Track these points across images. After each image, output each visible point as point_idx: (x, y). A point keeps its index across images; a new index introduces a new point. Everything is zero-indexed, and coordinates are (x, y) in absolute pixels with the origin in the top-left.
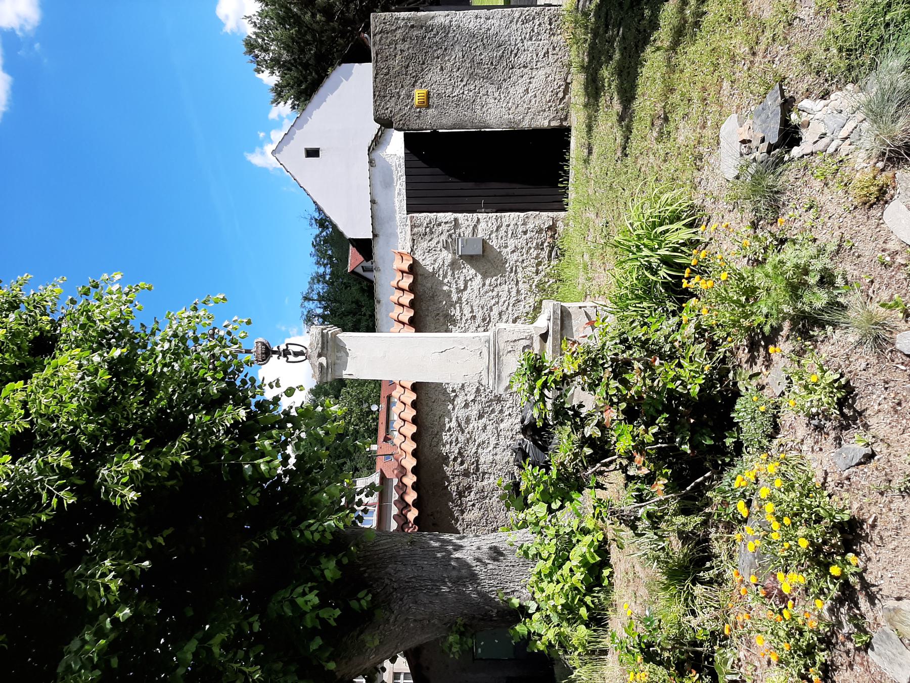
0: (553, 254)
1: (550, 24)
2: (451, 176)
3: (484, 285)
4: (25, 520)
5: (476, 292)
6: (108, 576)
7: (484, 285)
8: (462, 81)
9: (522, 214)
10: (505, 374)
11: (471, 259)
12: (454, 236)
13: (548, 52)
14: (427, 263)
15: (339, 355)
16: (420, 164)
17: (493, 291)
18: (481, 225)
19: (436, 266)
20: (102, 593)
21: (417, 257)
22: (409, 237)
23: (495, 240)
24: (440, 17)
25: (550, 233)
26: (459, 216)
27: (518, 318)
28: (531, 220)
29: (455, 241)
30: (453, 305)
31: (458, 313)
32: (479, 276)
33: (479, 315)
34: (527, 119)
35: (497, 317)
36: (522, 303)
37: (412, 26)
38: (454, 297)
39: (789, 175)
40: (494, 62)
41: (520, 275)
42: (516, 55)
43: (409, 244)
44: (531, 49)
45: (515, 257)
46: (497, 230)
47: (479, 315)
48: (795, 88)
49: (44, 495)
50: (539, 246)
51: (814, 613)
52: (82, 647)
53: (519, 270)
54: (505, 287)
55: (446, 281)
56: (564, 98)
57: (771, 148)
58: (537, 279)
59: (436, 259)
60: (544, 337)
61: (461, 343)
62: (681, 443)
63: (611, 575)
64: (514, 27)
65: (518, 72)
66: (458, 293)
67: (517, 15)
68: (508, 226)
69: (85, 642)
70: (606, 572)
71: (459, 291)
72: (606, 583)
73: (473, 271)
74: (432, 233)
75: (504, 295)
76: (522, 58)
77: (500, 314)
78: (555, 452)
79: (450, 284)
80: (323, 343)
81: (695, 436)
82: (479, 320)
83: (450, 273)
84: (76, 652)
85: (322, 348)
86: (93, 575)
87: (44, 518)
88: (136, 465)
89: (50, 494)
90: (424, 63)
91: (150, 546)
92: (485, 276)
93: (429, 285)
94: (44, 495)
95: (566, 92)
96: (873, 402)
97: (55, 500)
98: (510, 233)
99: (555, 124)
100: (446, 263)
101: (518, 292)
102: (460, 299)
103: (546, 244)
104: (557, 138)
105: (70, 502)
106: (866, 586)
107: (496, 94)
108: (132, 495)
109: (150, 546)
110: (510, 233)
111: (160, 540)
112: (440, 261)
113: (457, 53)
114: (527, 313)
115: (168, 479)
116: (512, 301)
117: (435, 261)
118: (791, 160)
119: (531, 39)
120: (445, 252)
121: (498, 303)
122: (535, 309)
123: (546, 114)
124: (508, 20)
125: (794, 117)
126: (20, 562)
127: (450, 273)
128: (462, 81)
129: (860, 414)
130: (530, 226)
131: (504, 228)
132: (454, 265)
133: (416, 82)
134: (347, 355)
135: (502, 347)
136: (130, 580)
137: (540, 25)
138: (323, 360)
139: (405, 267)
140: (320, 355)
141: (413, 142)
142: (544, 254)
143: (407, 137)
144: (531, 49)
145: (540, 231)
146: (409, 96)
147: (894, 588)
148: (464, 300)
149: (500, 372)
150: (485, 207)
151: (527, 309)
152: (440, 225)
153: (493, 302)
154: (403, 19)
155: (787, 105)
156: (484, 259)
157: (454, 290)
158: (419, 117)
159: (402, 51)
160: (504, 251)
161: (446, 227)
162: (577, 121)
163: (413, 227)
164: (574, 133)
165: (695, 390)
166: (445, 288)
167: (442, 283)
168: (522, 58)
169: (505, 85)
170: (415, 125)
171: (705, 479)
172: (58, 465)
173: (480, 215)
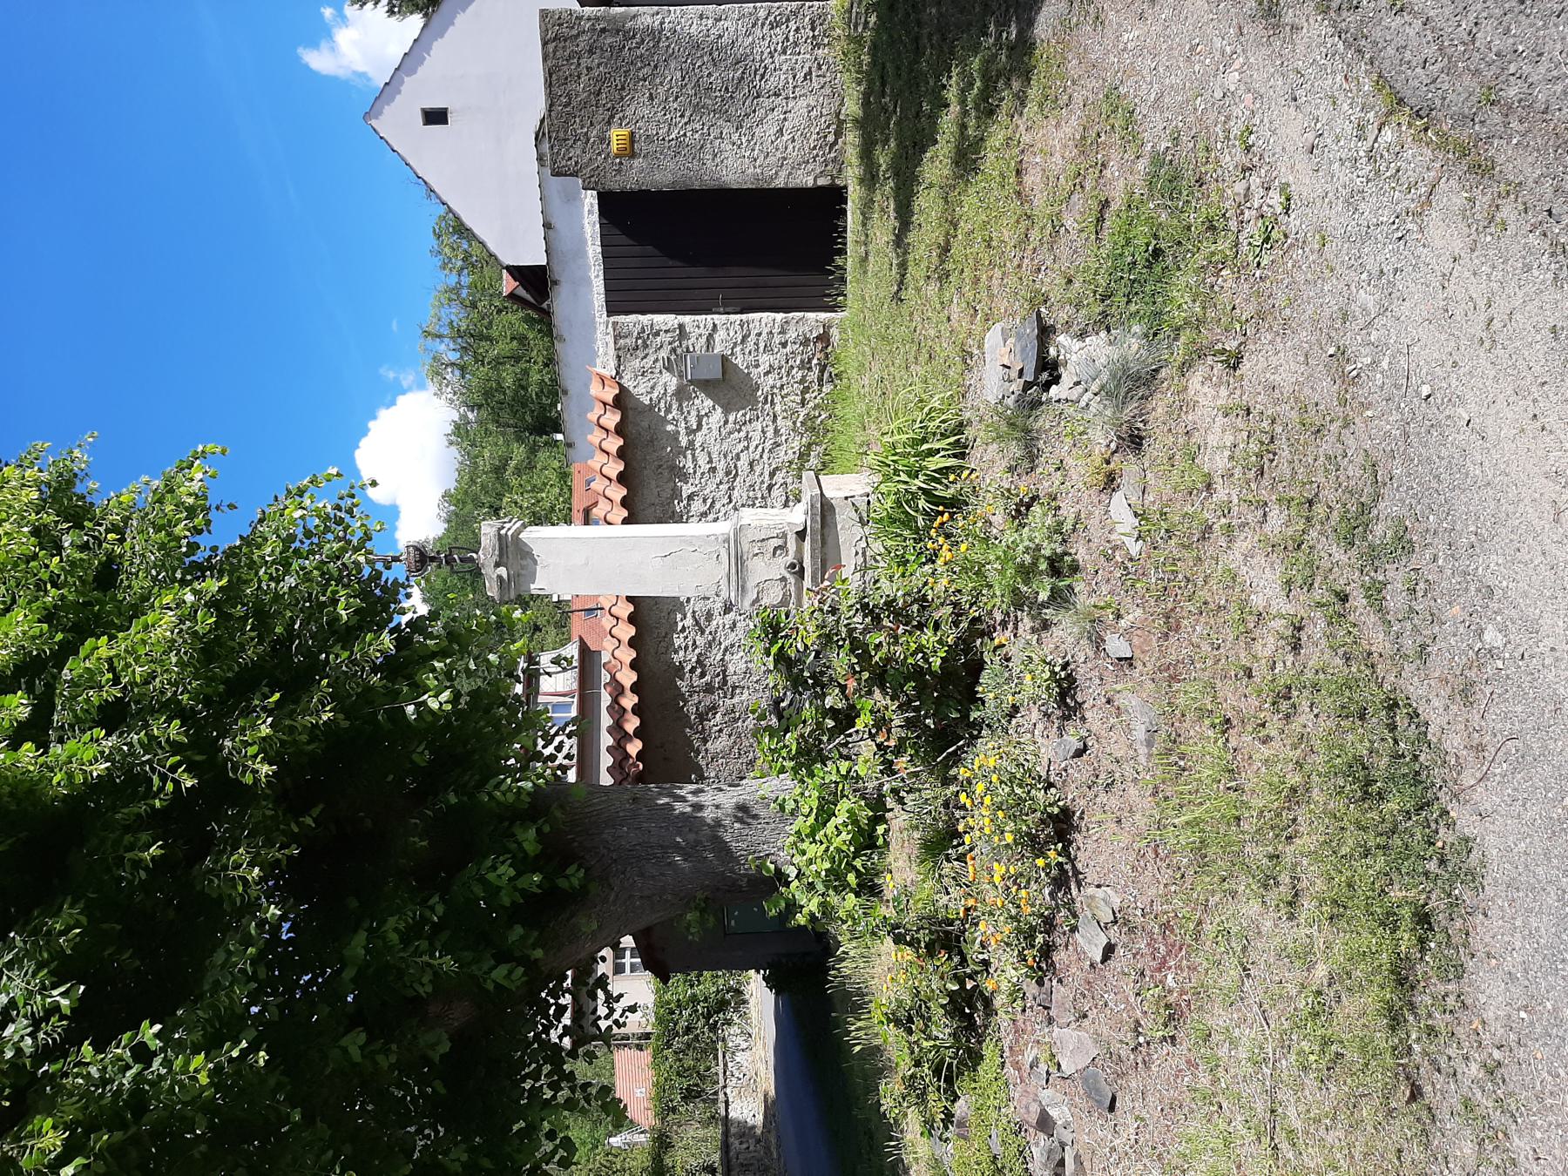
0: (826, 375)
1: (813, 29)
2: (672, 257)
3: (726, 422)
4: (136, 810)
5: (715, 432)
6: (245, 867)
7: (726, 422)
8: (682, 116)
9: (779, 316)
10: (750, 584)
11: (707, 386)
12: (679, 351)
13: (810, 73)
14: (640, 390)
15: (524, 563)
16: (624, 239)
17: (739, 431)
18: (720, 332)
19: (655, 395)
20: (240, 889)
21: (627, 382)
22: (612, 352)
23: (740, 357)
24: (646, 16)
25: (819, 346)
26: (687, 319)
27: (777, 469)
28: (792, 327)
29: (681, 359)
30: (682, 452)
31: (690, 464)
32: (719, 410)
33: (721, 466)
34: (783, 174)
35: (746, 468)
36: (783, 448)
37: (603, 30)
38: (684, 441)
39: (1043, 421)
40: (732, 88)
41: (778, 408)
42: (763, 76)
43: (612, 363)
44: (785, 68)
45: (770, 380)
46: (743, 341)
47: (721, 466)
48: (1058, 316)
49: (156, 779)
50: (806, 365)
51: (1036, 897)
52: (227, 960)
53: (777, 399)
54: (758, 425)
55: (670, 417)
56: (835, 142)
57: (1027, 386)
58: (803, 412)
59: (653, 385)
60: (801, 535)
61: (691, 544)
62: (926, 717)
63: (887, 831)
64: (759, 33)
65: (767, 103)
66: (688, 434)
67: (762, 14)
68: (759, 334)
69: (230, 953)
70: (880, 829)
71: (690, 432)
72: (880, 842)
73: (709, 403)
74: (646, 346)
75: (756, 437)
76: (772, 82)
77: (751, 464)
78: (808, 703)
79: (677, 422)
80: (501, 549)
81: (944, 707)
82: (720, 474)
83: (675, 407)
84: (223, 966)
85: (501, 555)
86: (225, 868)
87: (158, 803)
88: (265, 730)
89: (164, 778)
90: (623, 88)
91: (296, 830)
92: (727, 411)
93: (645, 424)
94: (156, 779)
95: (838, 134)
96: (1089, 693)
97: (170, 786)
98: (762, 345)
99: (822, 182)
100: (670, 391)
101: (776, 431)
102: (691, 443)
103: (815, 361)
104: (833, 197)
105: (189, 784)
106: (1076, 872)
107: (735, 137)
108: (265, 769)
109: (296, 830)
110: (762, 345)
111: (309, 821)
112: (660, 389)
113: (673, 74)
114: (791, 462)
115: (308, 743)
116: (768, 445)
117: (653, 388)
118: (1049, 401)
119: (784, 52)
120: (666, 376)
121: (747, 448)
122: (801, 456)
123: (810, 167)
124: (749, 21)
125: (1052, 352)
126: (137, 864)
127: (675, 407)
128: (682, 116)
129: (1080, 705)
130: (791, 335)
131: (752, 338)
132: (681, 394)
133: (612, 117)
134: (535, 562)
135: (745, 549)
136: (270, 869)
137: (797, 30)
138: (502, 571)
139: (609, 398)
140: (497, 565)
141: (615, 208)
142: (813, 376)
143: (599, 194)
144: (785, 68)
145: (806, 342)
146: (604, 139)
147: (1096, 876)
148: (697, 445)
149: (744, 582)
150: (724, 305)
151: (790, 456)
152: (657, 334)
153: (740, 447)
154: (589, 19)
155: (1045, 332)
156: (728, 385)
157: (683, 432)
158: (619, 171)
159: (589, 69)
160: (754, 372)
161: (666, 338)
162: (851, 178)
163: (617, 338)
164: (850, 189)
165: (936, 663)
166: (670, 428)
167: (664, 421)
168: (772, 82)
169: (747, 123)
170: (615, 184)
171: (959, 748)
172: (168, 740)
173: (719, 319)
